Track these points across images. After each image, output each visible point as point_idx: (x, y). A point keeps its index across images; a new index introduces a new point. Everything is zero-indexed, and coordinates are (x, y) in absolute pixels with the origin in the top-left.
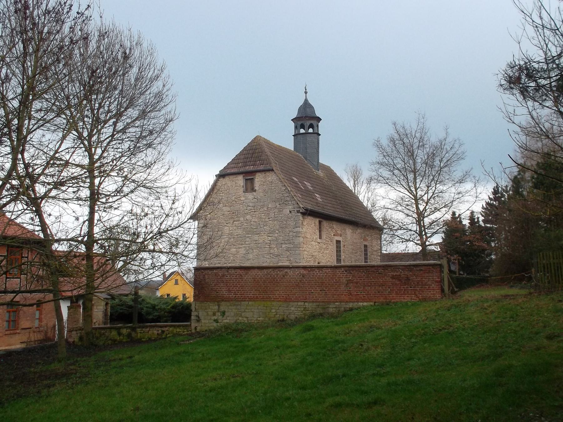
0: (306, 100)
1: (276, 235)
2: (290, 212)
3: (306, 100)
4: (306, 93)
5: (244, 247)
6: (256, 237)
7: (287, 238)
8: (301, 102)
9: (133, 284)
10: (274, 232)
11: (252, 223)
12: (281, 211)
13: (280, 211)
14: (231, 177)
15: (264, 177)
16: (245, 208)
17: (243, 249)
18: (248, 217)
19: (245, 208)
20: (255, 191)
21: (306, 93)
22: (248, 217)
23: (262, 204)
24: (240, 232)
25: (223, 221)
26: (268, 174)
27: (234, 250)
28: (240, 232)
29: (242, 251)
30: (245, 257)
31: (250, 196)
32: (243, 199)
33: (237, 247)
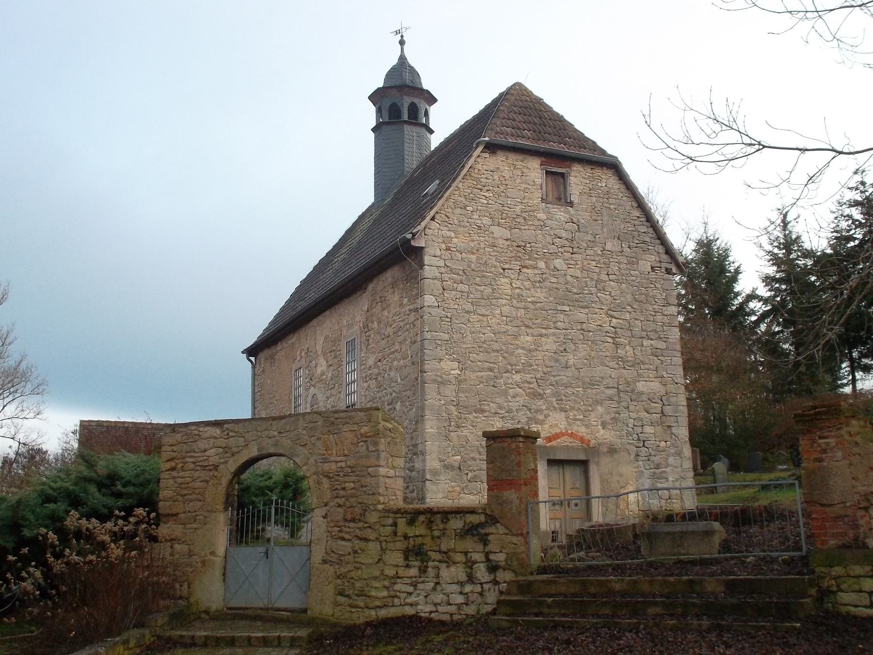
0: (402, 59)
1: (628, 316)
2: (652, 268)
3: (402, 59)
4: (402, 43)
5: (554, 335)
6: (581, 315)
7: (652, 326)
8: (395, 61)
9: (308, 417)
10: (621, 308)
11: (569, 278)
12: (633, 263)
13: (633, 262)
14: (512, 157)
15: (592, 179)
16: (549, 239)
17: (551, 339)
18: (558, 263)
19: (549, 239)
20: (571, 204)
21: (402, 43)
22: (558, 263)
23: (590, 237)
24: (540, 294)
25: (493, 261)
26: (598, 172)
27: (529, 338)
28: (540, 294)
29: (549, 344)
30: (557, 361)
31: (560, 214)
32: (542, 216)
33: (536, 331)
